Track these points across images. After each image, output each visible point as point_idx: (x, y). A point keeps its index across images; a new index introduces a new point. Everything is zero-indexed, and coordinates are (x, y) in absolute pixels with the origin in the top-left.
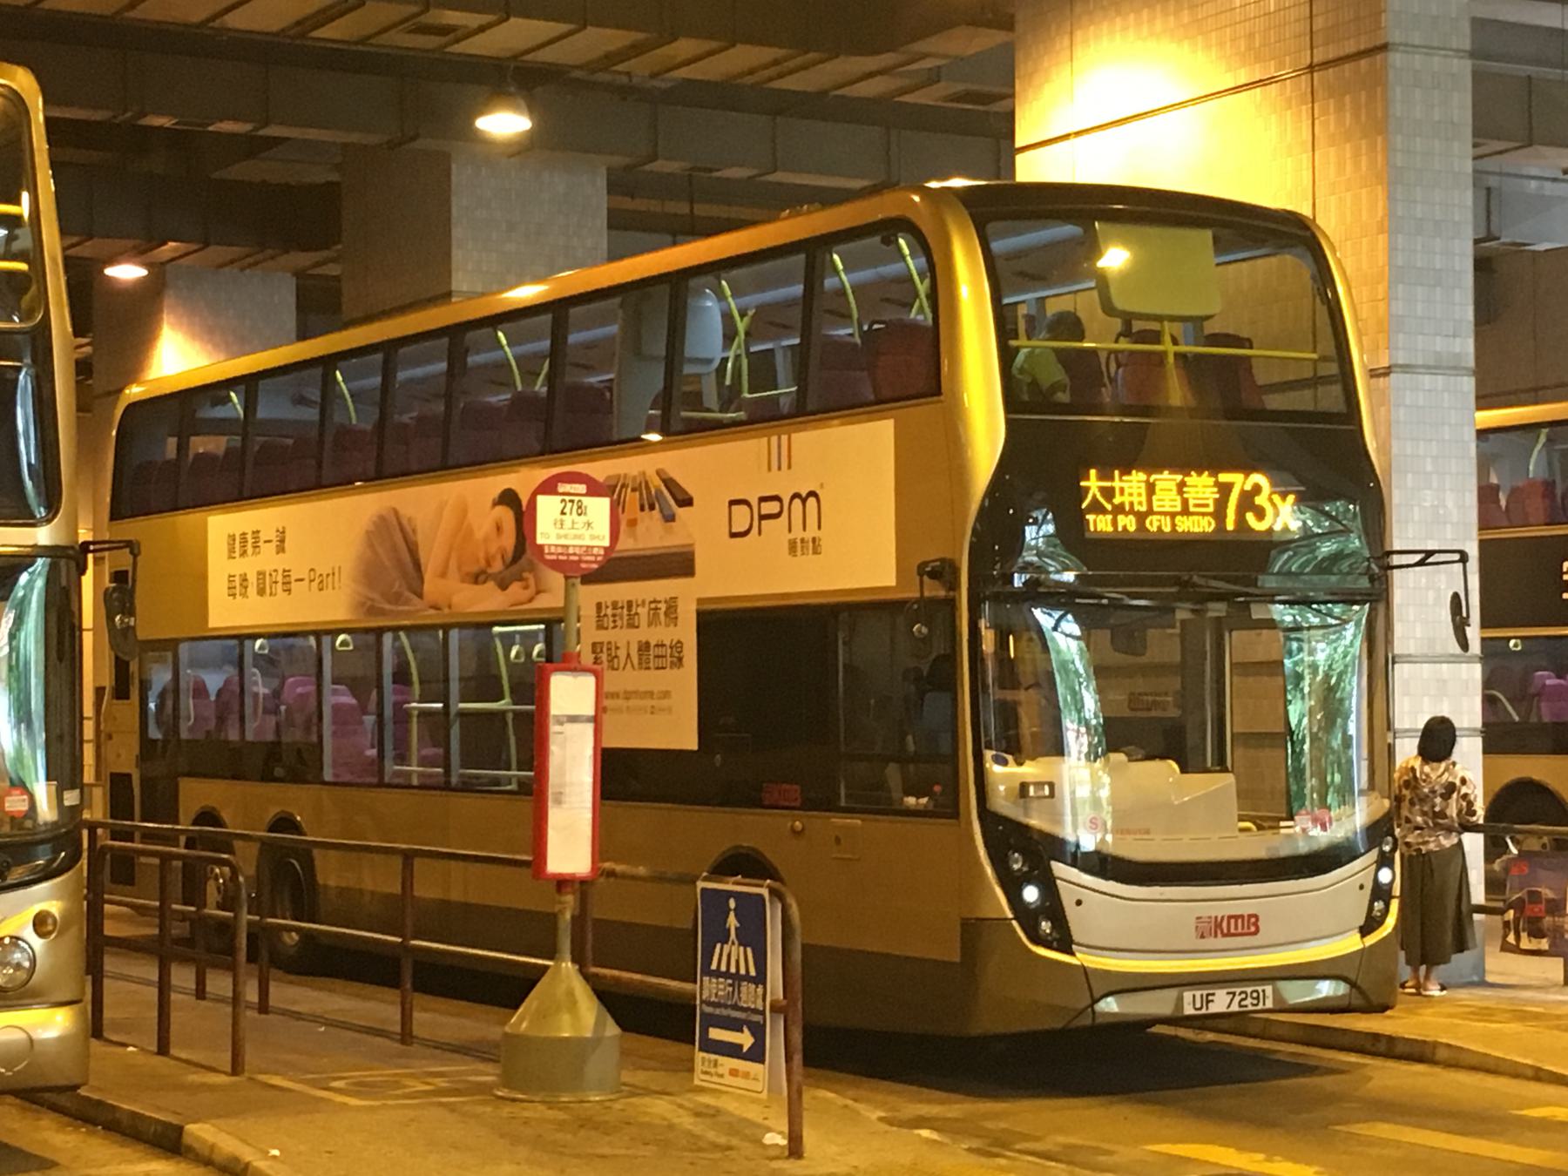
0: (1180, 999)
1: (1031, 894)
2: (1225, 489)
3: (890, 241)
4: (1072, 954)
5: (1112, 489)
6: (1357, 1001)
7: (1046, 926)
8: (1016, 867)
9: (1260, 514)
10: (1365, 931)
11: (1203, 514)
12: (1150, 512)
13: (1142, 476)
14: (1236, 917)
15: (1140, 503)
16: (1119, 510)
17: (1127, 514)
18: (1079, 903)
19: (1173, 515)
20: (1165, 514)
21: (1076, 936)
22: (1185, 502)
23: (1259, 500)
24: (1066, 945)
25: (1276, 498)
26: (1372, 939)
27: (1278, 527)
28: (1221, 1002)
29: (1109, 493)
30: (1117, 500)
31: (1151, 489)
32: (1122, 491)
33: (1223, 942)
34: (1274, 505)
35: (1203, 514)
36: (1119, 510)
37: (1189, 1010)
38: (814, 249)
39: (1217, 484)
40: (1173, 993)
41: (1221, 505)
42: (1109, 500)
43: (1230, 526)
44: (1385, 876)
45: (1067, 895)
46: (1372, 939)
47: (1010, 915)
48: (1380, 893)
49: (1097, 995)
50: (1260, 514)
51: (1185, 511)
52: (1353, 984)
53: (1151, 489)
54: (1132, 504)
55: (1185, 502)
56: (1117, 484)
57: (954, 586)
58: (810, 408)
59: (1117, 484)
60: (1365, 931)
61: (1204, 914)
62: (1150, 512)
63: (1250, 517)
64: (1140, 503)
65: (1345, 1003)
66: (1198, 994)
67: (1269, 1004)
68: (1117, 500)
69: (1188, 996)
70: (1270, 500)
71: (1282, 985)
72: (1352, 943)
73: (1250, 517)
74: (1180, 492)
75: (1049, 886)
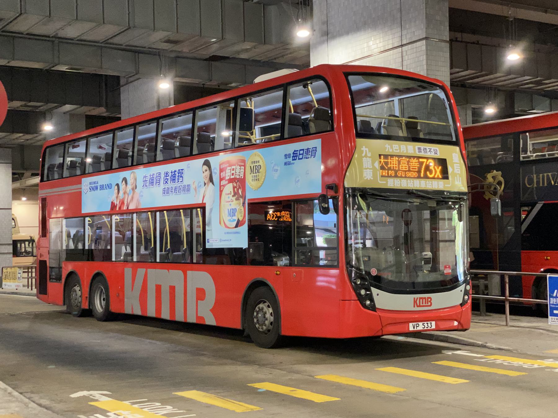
1: (363, 292)
2: (421, 163)
5: (388, 162)
6: (460, 328)
7: (368, 302)
8: (359, 283)
9: (431, 172)
11: (414, 171)
12: (399, 170)
13: (397, 159)
15: (396, 167)
16: (389, 169)
17: (392, 170)
18: (378, 295)
19: (405, 171)
20: (403, 171)
21: (377, 306)
22: (409, 167)
23: (432, 168)
25: (436, 167)
27: (436, 176)
28: (421, 327)
29: (387, 163)
30: (389, 166)
31: (399, 163)
32: (391, 162)
34: (435, 169)
35: (414, 171)
36: (389, 169)
39: (419, 162)
41: (420, 169)
42: (387, 166)
50: (431, 173)
51: (409, 171)
53: (399, 163)
54: (393, 167)
55: (409, 167)
56: (389, 161)
59: (389, 161)
62: (399, 170)
63: (428, 173)
64: (396, 167)
65: (456, 328)
68: (389, 166)
70: (434, 168)
73: (428, 173)
74: (408, 164)
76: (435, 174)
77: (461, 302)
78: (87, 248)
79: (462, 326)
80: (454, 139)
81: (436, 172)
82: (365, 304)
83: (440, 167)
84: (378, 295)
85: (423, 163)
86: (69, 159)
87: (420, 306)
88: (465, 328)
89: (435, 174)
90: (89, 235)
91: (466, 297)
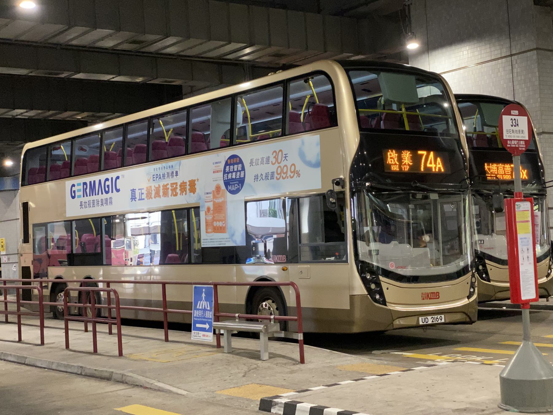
0: (418, 320)
1: (373, 286)
3: (306, 81)
4: (386, 305)
6: (468, 320)
7: (378, 297)
8: (368, 277)
10: (469, 297)
14: (433, 293)
18: (387, 289)
21: (387, 300)
24: (384, 303)
26: (472, 299)
28: (430, 320)
33: (428, 301)
37: (421, 323)
38: (285, 83)
40: (416, 318)
44: (473, 280)
45: (384, 286)
46: (472, 299)
47: (366, 293)
48: (472, 285)
49: (394, 318)
52: (466, 314)
57: (343, 187)
58: (286, 134)
60: (469, 297)
61: (424, 292)
66: (423, 318)
67: (443, 321)
69: (420, 318)
71: (447, 315)
72: (465, 301)
75: (378, 284)
77: (468, 295)
78: (74, 252)
79: (470, 318)
84: (387, 289)
91: (472, 290)
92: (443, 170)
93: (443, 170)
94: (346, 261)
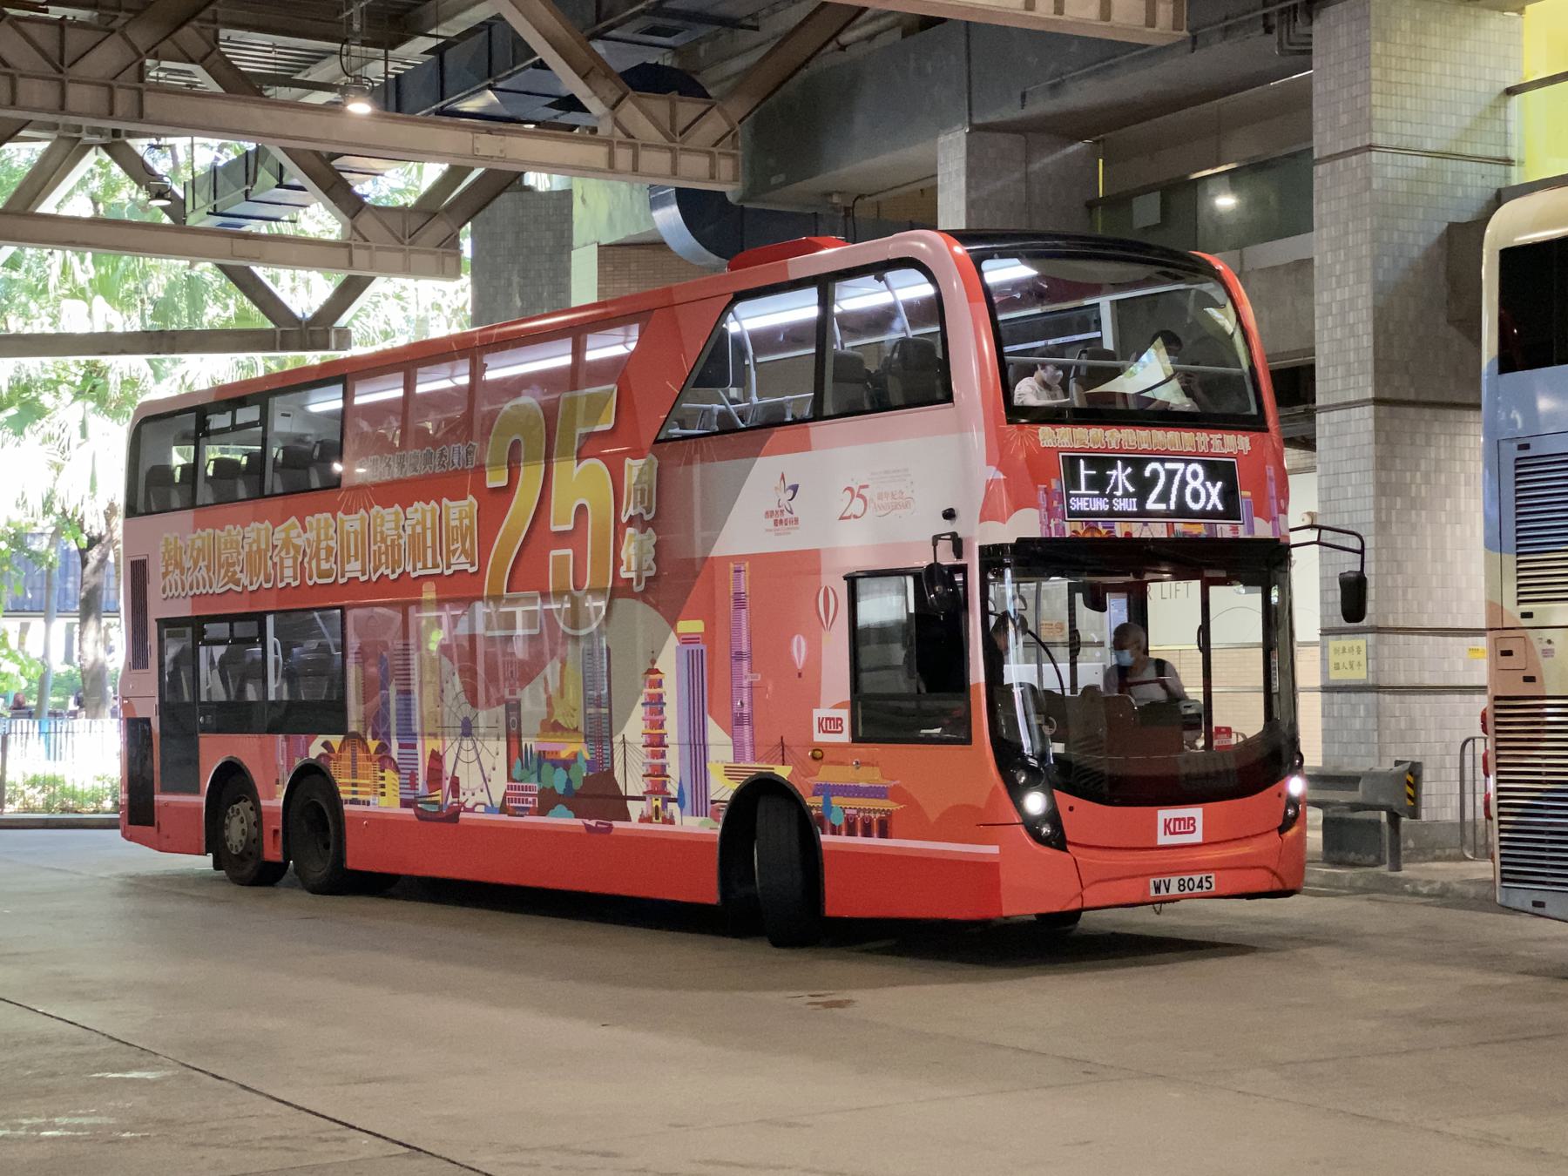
2: (1171, 474)
25: (1208, 484)
27: (1209, 507)
40: (1141, 880)
43: (1173, 506)
50: (1196, 496)
70: (1204, 485)
76: (1207, 501)
78: (272, 697)
80: (1254, 411)
81: (1208, 496)
82: (1040, 832)
83: (1219, 484)
84: (1071, 809)
85: (1174, 472)
86: (213, 453)
87: (1175, 833)
88: (1289, 886)
89: (1207, 501)
90: (277, 662)
92: (1220, 507)
93: (1220, 507)
94: (968, 741)
